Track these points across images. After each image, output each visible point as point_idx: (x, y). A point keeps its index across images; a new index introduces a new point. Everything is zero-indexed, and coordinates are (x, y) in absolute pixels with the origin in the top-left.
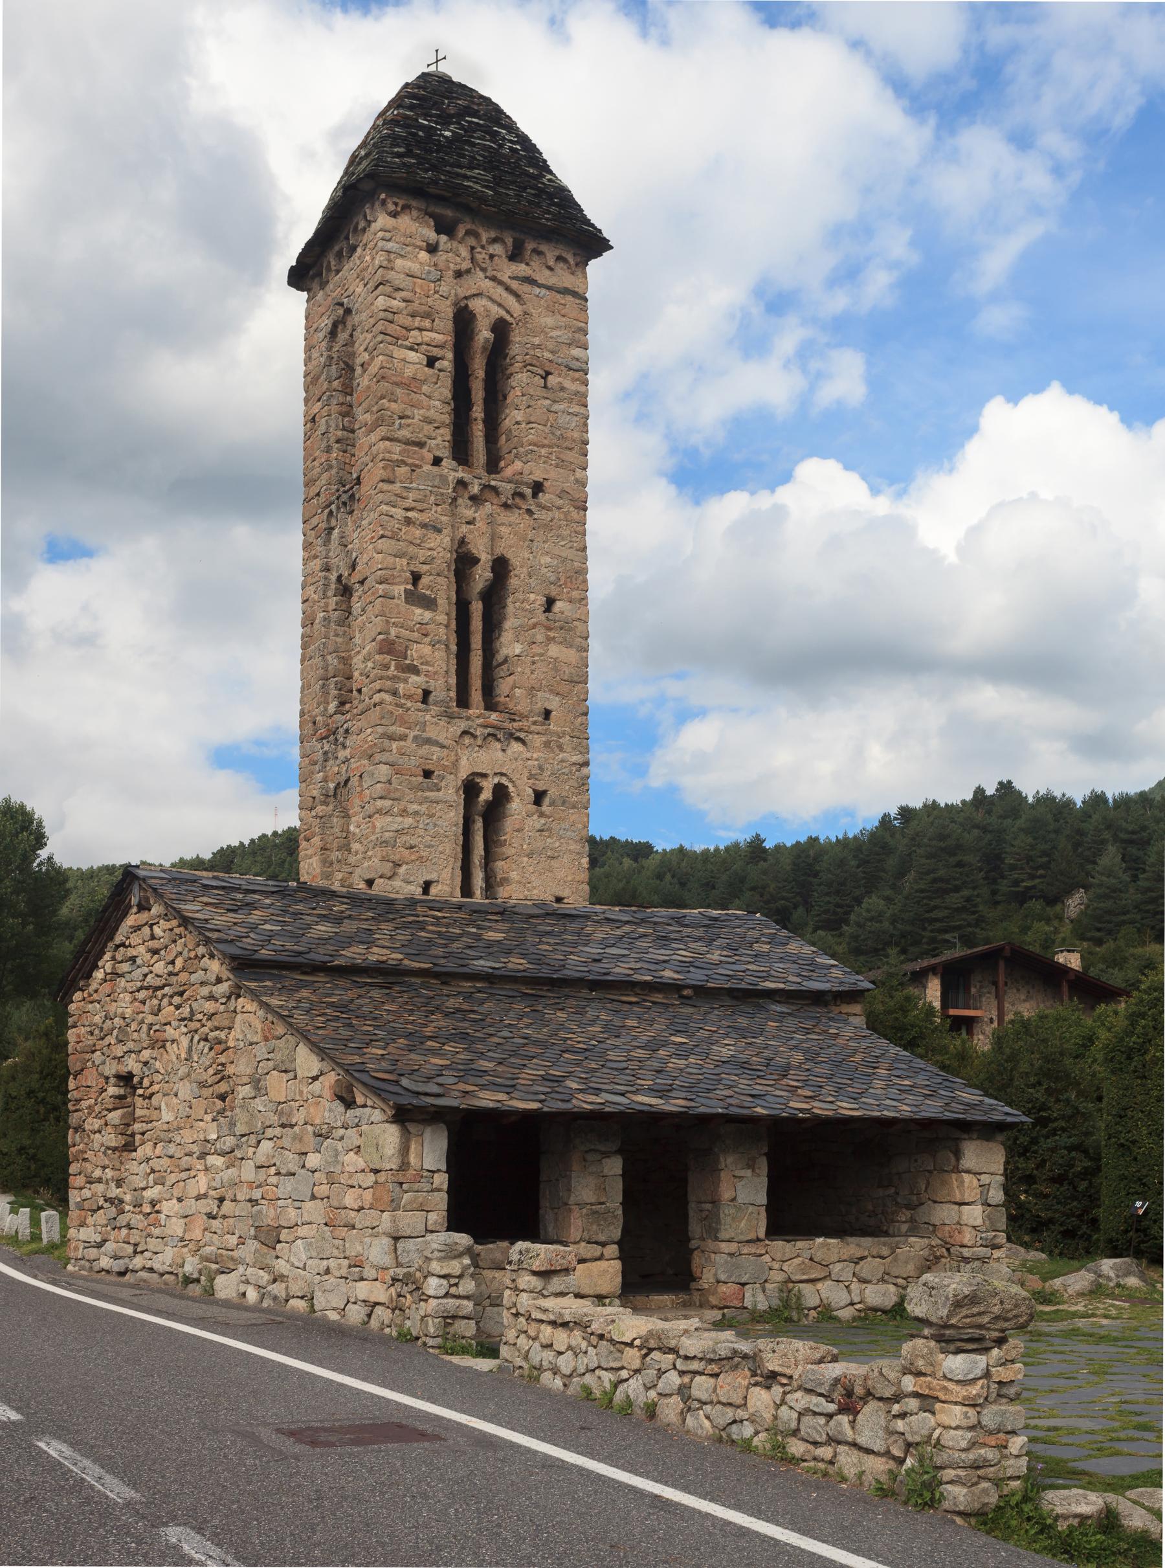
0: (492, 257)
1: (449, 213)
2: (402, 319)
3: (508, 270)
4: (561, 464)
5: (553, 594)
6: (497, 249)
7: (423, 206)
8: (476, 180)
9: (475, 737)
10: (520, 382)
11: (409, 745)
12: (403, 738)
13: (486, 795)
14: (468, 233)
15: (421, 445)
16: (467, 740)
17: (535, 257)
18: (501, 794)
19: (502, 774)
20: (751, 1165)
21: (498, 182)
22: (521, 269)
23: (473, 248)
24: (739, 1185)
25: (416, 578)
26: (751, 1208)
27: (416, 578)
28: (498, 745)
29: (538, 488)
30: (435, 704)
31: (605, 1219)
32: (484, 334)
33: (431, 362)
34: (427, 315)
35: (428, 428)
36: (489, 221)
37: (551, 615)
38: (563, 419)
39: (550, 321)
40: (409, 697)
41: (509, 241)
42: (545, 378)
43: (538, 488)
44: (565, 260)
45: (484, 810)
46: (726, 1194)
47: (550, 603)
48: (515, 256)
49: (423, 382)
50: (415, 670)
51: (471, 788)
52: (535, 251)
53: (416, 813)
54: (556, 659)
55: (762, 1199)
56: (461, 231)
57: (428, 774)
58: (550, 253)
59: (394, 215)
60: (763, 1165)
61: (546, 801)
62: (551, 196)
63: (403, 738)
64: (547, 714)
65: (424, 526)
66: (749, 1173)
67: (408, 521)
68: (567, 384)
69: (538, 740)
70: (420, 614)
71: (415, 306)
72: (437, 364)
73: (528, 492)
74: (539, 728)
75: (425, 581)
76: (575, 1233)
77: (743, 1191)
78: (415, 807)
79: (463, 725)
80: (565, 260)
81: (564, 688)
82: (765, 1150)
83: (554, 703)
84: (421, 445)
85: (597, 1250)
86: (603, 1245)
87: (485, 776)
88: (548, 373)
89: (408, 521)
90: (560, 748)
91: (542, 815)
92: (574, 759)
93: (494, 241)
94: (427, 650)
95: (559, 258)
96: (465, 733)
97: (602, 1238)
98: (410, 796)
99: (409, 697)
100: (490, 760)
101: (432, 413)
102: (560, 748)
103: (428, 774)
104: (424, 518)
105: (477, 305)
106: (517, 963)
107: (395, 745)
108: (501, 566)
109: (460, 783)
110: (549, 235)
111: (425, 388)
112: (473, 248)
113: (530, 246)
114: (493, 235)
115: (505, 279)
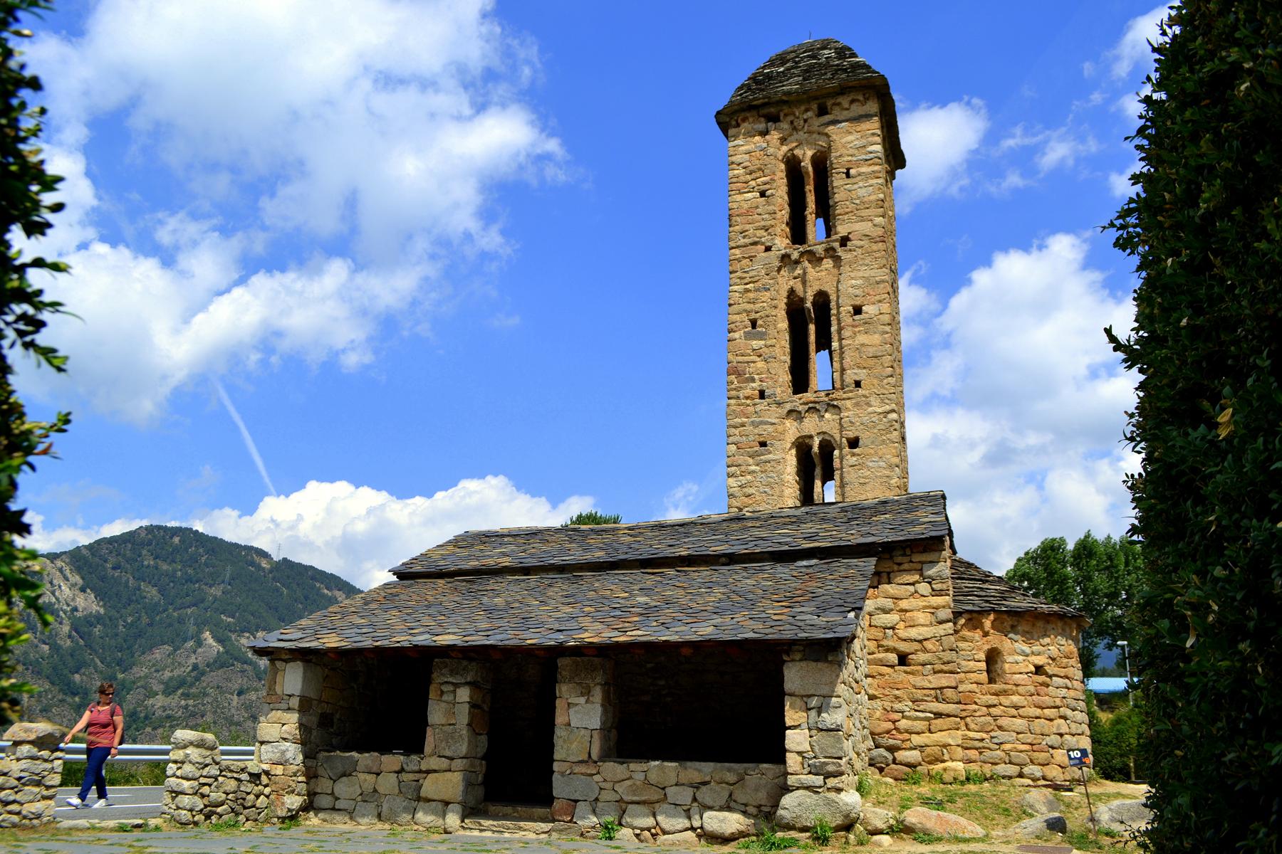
0: (805, 121)
1: (772, 110)
2: (742, 179)
3: (817, 122)
4: (862, 219)
5: (858, 303)
6: (809, 114)
7: (754, 113)
8: (790, 84)
9: (800, 412)
10: (837, 181)
11: (749, 428)
12: (743, 425)
13: (816, 449)
14: (786, 115)
15: (755, 243)
16: (794, 415)
17: (837, 108)
18: (827, 448)
19: (824, 433)
20: (587, 692)
21: (804, 79)
22: (827, 118)
23: (792, 122)
24: (572, 711)
25: (754, 324)
26: (583, 732)
27: (754, 324)
28: (815, 416)
29: (844, 241)
30: (769, 397)
31: (452, 738)
32: (807, 164)
33: (763, 194)
34: (760, 169)
35: (762, 233)
36: (798, 102)
37: (857, 317)
38: (861, 192)
39: (850, 138)
40: (747, 398)
41: (815, 107)
42: (848, 175)
43: (844, 241)
44: (858, 100)
45: (815, 463)
46: (560, 719)
47: (858, 310)
48: (823, 111)
49: (757, 207)
50: (753, 380)
51: (802, 447)
52: (834, 104)
53: (754, 472)
54: (863, 345)
55: (596, 723)
56: (782, 115)
57: (763, 444)
58: (845, 101)
59: (738, 125)
60: (598, 695)
61: (861, 443)
62: (845, 71)
63: (743, 425)
64: (858, 384)
65: (757, 290)
66: (582, 700)
67: (747, 291)
68: (863, 169)
69: (848, 403)
70: (756, 344)
71: (752, 168)
72: (768, 193)
73: (836, 245)
74: (850, 395)
75: (760, 322)
76: (428, 748)
77: (580, 718)
78: (753, 468)
79: (788, 407)
80: (858, 100)
81: (871, 362)
82: (598, 680)
83: (862, 375)
84: (755, 243)
85: (444, 763)
86: (452, 759)
87: (811, 437)
88: (848, 170)
89: (747, 291)
90: (869, 405)
91: (854, 455)
92: (880, 410)
93: (807, 110)
94: (761, 365)
95: (852, 102)
96: (790, 412)
97: (448, 753)
98: (751, 461)
99: (747, 398)
100: (811, 425)
101: (763, 223)
102: (869, 405)
103: (763, 444)
104: (759, 284)
105: (798, 152)
106: (599, 555)
107: (737, 432)
108: (822, 301)
109: (789, 445)
110: (843, 90)
111: (759, 211)
112: (792, 122)
113: (829, 103)
114: (803, 108)
115: (816, 128)
